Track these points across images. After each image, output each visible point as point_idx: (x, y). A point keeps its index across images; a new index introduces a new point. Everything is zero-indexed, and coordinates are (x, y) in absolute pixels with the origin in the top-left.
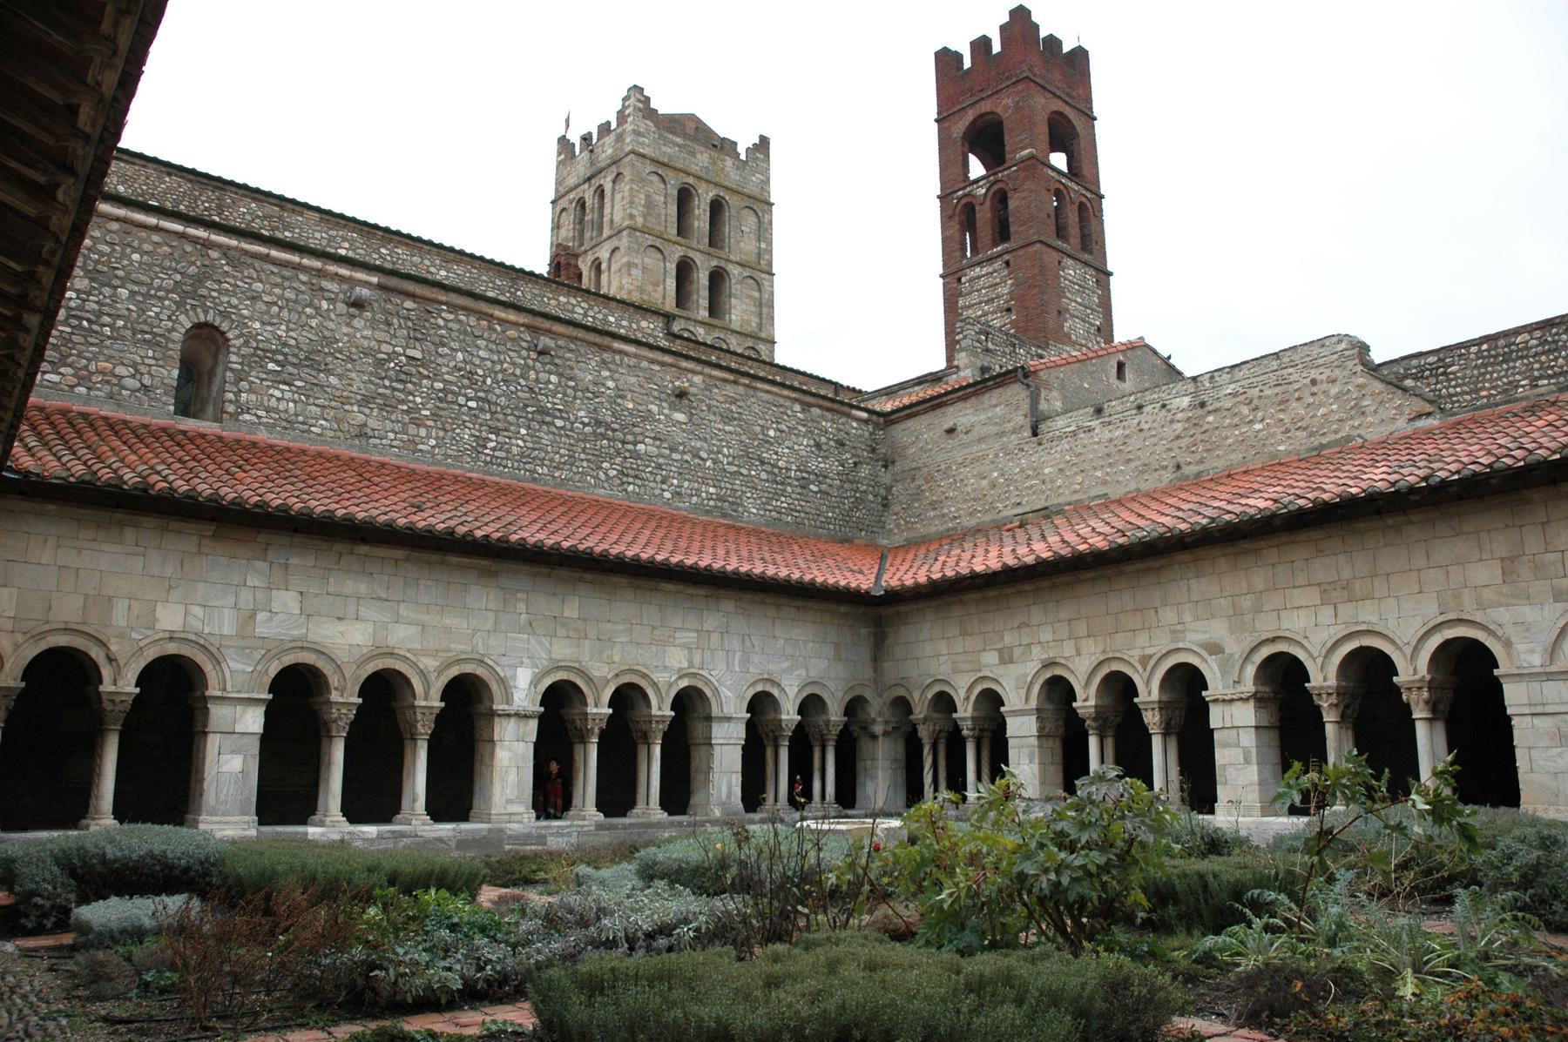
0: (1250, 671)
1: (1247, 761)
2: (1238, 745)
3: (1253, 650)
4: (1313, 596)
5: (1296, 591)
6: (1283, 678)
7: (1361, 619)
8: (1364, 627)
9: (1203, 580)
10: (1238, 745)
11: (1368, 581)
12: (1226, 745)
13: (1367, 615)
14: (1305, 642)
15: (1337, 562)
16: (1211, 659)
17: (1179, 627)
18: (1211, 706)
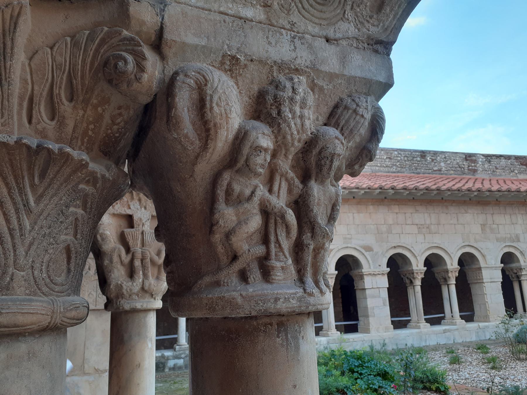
0: (385, 261)
1: (384, 304)
2: (379, 297)
3: (387, 251)
4: (415, 229)
5: (407, 226)
6: (397, 265)
7: (435, 241)
8: (436, 245)
9: (361, 215)
10: (379, 297)
11: (436, 226)
12: (373, 297)
13: (437, 240)
14: (412, 249)
15: (423, 216)
16: (366, 254)
17: (348, 236)
18: (365, 277)
